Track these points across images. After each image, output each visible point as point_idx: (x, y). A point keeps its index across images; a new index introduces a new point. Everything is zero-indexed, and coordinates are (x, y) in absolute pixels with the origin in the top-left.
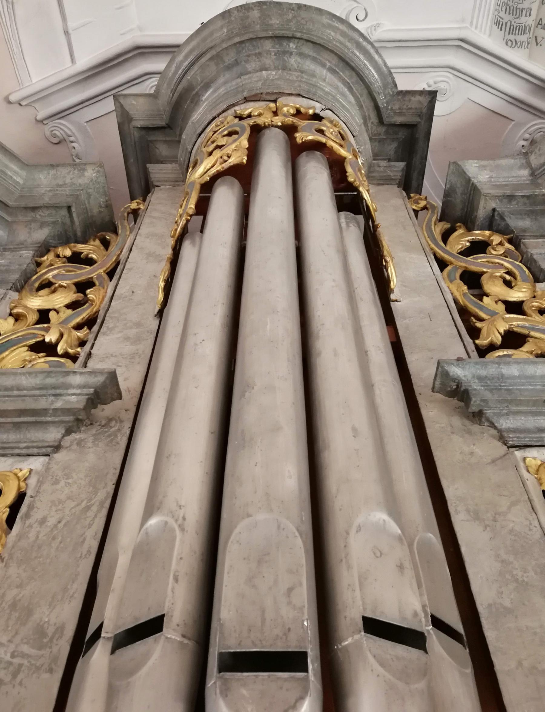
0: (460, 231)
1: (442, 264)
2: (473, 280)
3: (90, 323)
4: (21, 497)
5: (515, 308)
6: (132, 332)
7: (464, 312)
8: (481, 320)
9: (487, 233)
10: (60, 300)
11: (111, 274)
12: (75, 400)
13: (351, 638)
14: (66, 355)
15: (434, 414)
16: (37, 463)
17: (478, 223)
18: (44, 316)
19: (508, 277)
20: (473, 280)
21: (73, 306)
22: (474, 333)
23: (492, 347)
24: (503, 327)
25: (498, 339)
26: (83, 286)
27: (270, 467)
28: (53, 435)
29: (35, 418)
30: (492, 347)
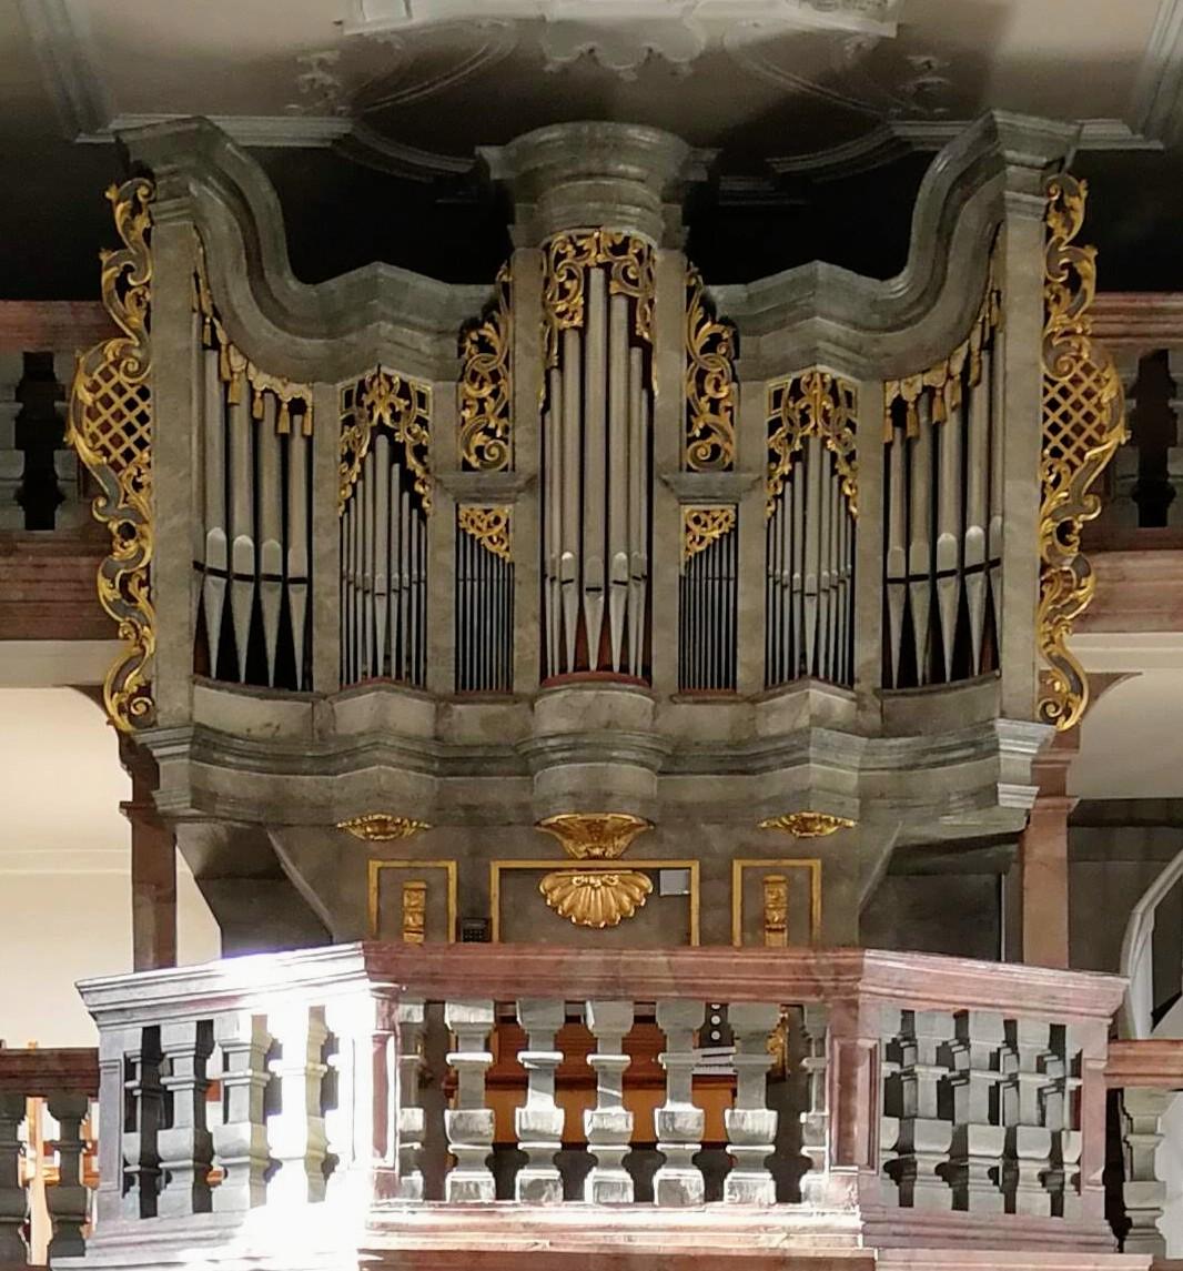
0: (708, 324)
1: (690, 360)
2: (701, 376)
3: (504, 414)
4: (508, 521)
5: (715, 405)
6: (530, 426)
7: (690, 411)
8: (696, 416)
9: (722, 327)
10: (486, 391)
11: (506, 362)
12: (520, 483)
13: (611, 584)
14: (501, 438)
15: (657, 485)
16: (511, 506)
17: (717, 319)
18: (482, 401)
19: (720, 377)
20: (701, 376)
21: (495, 394)
22: (690, 427)
23: (694, 439)
24: (701, 425)
25: (698, 433)
26: (495, 376)
27: (594, 542)
28: (513, 494)
29: (509, 490)
30: (694, 439)
